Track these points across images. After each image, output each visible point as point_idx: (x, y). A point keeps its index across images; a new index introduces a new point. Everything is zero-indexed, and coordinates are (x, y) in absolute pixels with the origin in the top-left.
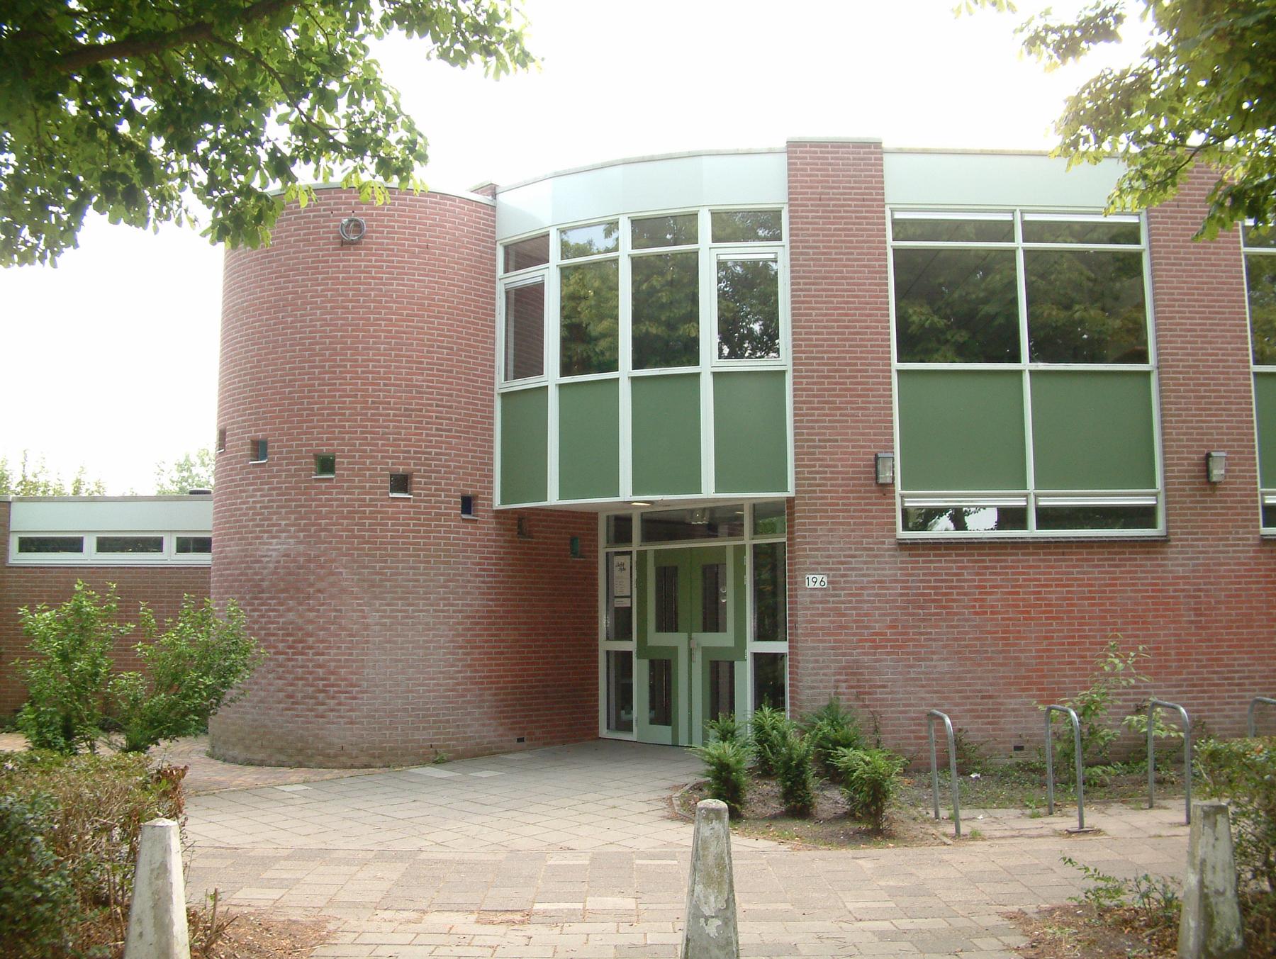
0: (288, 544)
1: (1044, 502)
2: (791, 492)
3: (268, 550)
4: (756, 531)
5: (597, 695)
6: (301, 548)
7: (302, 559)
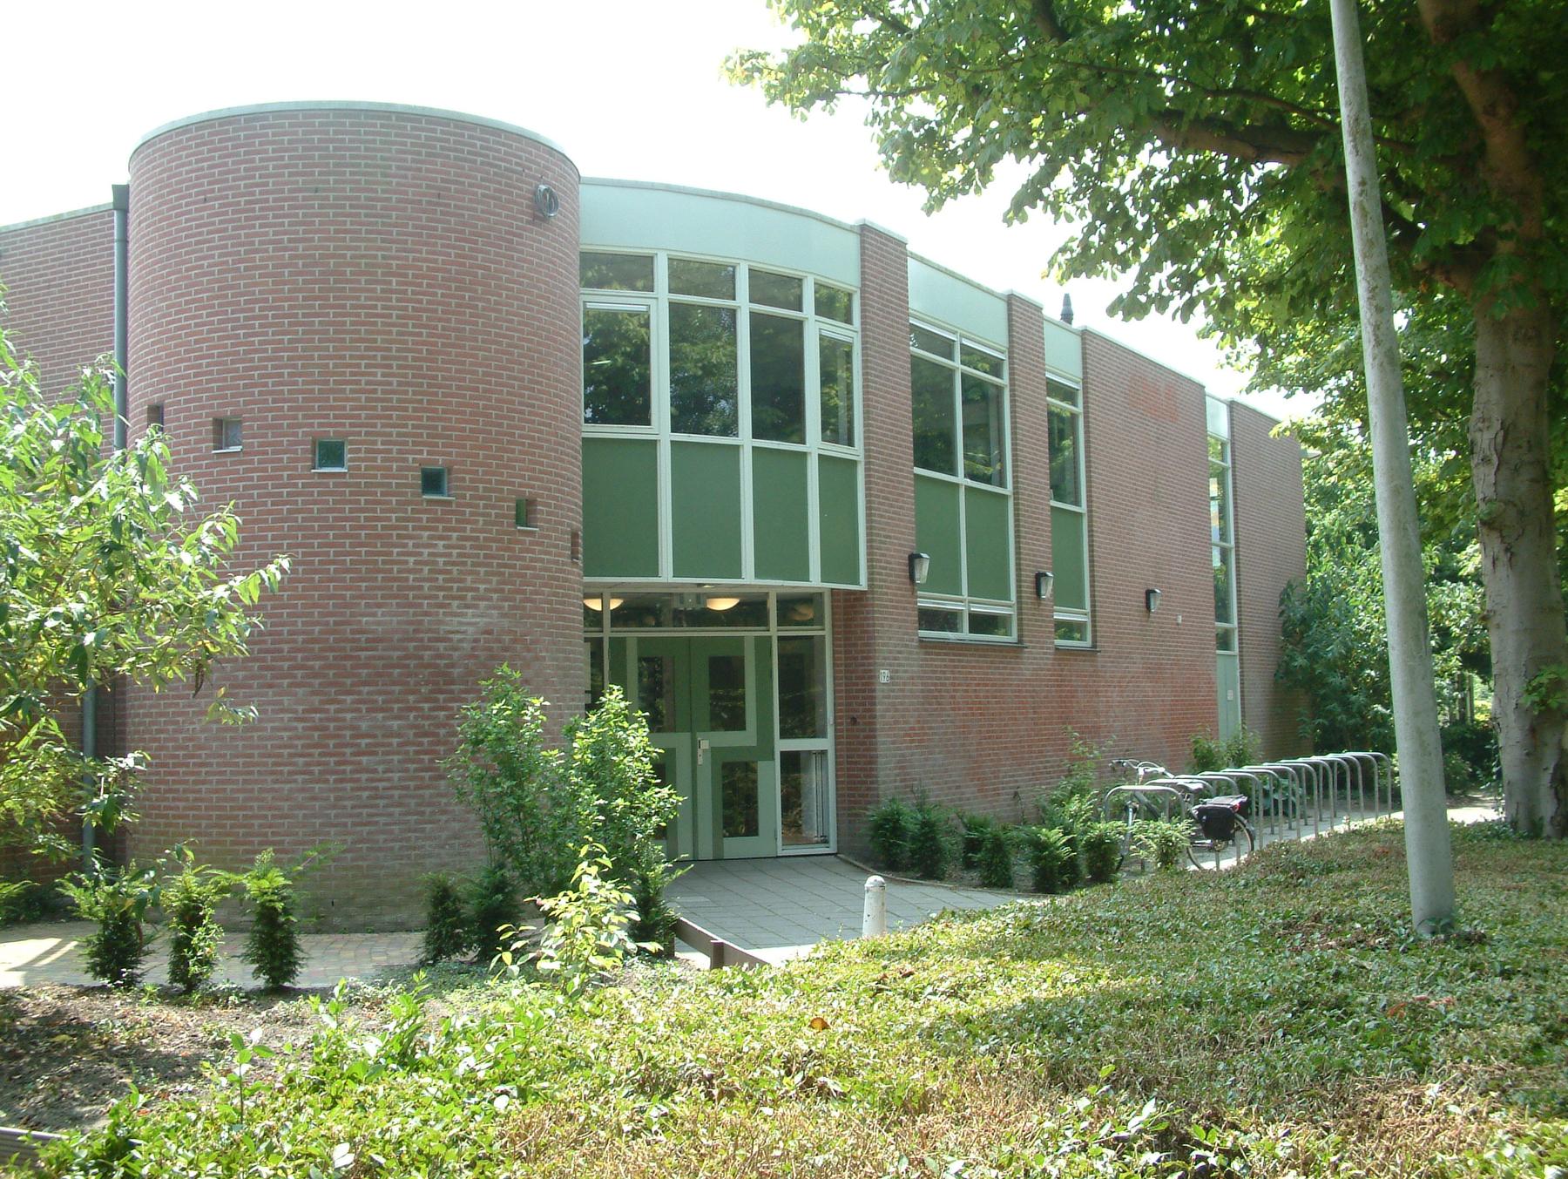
0: (491, 616)
1: (976, 609)
2: (863, 585)
3: (460, 623)
4: (783, 620)
5: (838, 796)
6: (506, 622)
7: (507, 638)
